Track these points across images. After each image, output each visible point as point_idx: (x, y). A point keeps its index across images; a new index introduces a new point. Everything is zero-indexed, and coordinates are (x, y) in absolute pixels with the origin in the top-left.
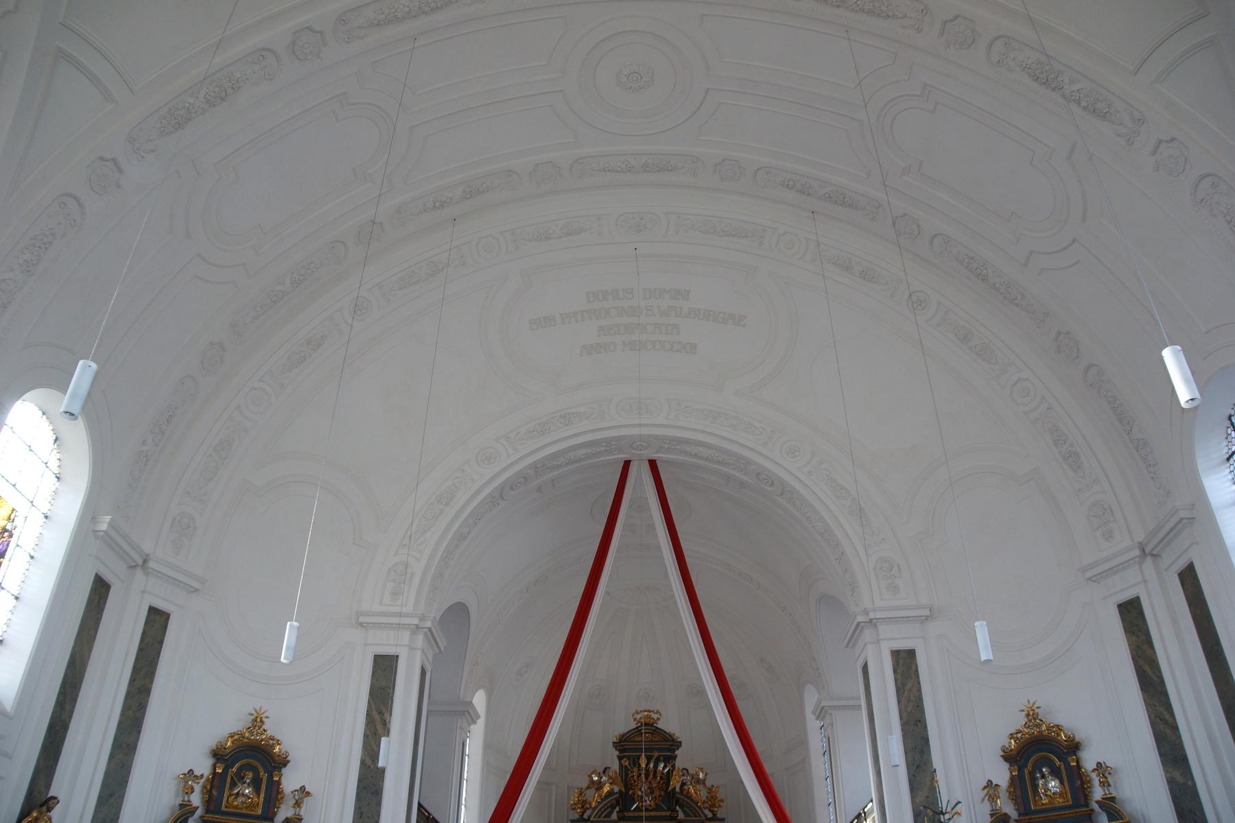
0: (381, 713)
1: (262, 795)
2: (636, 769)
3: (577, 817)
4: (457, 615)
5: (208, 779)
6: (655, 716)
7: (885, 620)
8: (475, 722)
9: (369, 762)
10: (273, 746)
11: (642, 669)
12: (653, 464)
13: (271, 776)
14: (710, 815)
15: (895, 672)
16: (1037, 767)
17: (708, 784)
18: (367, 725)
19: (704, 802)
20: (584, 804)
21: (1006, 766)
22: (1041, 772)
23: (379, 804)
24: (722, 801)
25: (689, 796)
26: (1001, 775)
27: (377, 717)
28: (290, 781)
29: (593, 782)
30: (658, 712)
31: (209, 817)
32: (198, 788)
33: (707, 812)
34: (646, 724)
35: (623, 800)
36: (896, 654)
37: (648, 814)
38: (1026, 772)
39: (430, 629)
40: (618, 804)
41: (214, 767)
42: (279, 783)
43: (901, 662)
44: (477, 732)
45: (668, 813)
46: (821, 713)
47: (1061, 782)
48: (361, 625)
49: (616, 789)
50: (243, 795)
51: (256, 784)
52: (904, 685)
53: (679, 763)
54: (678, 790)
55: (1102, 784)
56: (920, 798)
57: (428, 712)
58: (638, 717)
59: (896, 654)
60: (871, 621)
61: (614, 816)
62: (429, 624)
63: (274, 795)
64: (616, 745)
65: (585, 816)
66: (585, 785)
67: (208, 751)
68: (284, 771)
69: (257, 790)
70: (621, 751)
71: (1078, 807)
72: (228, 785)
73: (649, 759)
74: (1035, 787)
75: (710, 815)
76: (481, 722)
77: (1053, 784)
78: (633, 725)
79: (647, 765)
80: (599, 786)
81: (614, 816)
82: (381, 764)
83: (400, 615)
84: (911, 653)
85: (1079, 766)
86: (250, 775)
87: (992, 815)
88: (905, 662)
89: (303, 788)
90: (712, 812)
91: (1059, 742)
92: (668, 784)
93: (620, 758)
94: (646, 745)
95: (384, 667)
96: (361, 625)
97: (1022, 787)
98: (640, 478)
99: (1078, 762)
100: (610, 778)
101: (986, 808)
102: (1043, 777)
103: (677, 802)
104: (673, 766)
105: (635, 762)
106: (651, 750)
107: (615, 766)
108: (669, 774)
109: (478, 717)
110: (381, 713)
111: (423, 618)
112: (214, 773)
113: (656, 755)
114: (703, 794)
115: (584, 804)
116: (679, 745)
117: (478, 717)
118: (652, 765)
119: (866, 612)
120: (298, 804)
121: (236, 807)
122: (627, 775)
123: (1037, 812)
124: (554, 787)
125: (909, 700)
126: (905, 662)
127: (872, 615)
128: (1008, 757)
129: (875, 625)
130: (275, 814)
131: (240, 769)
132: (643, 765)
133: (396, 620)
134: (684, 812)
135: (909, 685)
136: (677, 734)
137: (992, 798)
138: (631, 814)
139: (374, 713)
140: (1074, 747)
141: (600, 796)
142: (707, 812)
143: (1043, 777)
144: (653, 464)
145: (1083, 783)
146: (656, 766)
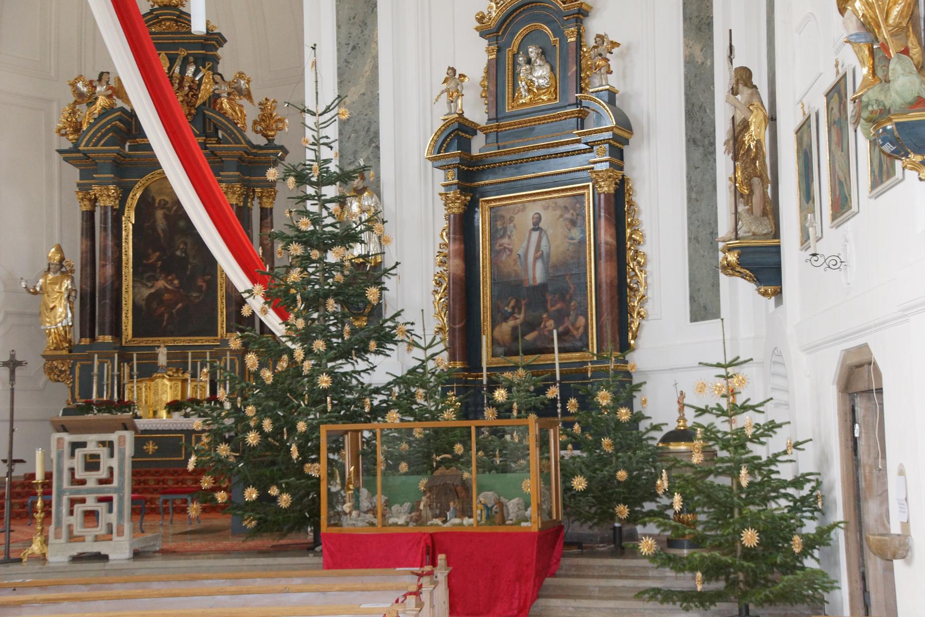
3: (67, 145)
14: (262, 141)
17: (258, 97)
20: (77, 129)
22: (526, 54)
26: (475, 58)
29: (80, 95)
47: (552, 69)
56: (353, 95)
66: (72, 99)
73: (172, 60)
79: (170, 69)
80: (91, 100)
85: (579, 44)
90: (266, 136)
99: (580, 36)
102: (529, 62)
106: (176, 46)
113: (183, 53)
114: (251, 112)
118: (177, 70)
141: (91, 114)
146: (183, 71)
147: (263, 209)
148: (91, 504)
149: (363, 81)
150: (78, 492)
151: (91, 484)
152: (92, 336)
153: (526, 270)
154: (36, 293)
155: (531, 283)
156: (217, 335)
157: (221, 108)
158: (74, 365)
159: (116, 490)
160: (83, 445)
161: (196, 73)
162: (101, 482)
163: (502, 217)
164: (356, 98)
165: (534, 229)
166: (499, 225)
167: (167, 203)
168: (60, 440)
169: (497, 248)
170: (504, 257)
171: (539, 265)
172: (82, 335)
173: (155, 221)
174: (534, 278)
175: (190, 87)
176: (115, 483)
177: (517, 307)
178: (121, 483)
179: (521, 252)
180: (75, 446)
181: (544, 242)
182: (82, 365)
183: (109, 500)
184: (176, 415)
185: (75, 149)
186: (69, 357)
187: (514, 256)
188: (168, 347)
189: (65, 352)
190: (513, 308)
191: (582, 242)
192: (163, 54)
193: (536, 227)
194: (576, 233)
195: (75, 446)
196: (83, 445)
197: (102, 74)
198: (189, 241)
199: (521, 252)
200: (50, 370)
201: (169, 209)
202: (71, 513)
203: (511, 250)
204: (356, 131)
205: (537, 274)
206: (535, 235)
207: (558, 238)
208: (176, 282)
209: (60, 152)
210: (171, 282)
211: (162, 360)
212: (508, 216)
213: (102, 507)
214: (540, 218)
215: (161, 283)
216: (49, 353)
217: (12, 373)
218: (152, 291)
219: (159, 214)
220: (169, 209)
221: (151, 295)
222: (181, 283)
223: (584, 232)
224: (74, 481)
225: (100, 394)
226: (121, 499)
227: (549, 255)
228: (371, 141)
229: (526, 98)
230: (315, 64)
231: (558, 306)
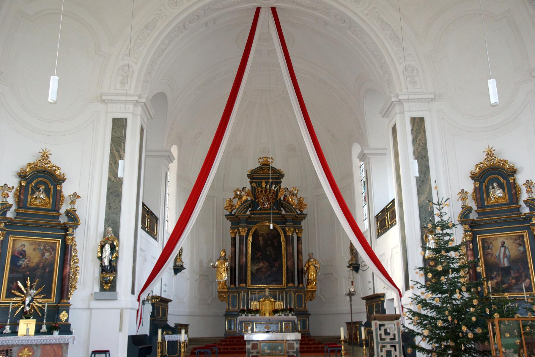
0: (118, 151)
1: (51, 198)
2: (259, 188)
3: (228, 213)
4: (160, 99)
5: (17, 190)
6: (270, 160)
7: (408, 100)
8: (172, 162)
9: (113, 179)
10: (55, 171)
11: (265, 133)
12: (274, 10)
13: (55, 187)
14: (299, 212)
15: (412, 129)
16: (491, 182)
17: (299, 196)
18: (110, 158)
19: (296, 206)
21: (473, 181)
22: (492, 185)
23: (120, 201)
24: (306, 205)
25: (288, 202)
26: (470, 186)
27: (116, 154)
28: (67, 190)
30: (272, 158)
31: (20, 211)
32: (11, 194)
33: (297, 210)
34: (266, 165)
35: (253, 204)
36: (413, 120)
37: (269, 212)
38: (484, 185)
39: (144, 103)
40: (250, 207)
41: (21, 184)
42: (61, 191)
43: (416, 124)
44: (173, 167)
45: (277, 211)
46: (363, 157)
47: (504, 191)
48: (104, 101)
49: (249, 199)
50: (39, 198)
51: (47, 192)
52: (416, 137)
53: (283, 186)
54: (282, 199)
55: (528, 192)
56: (423, 198)
57: (146, 156)
58: (261, 161)
59: (413, 120)
60: (400, 100)
61: (248, 213)
62: (144, 100)
63: (57, 198)
64: (249, 176)
65: (233, 213)
67: (16, 174)
68: (63, 184)
69: (48, 195)
70: (251, 179)
71: (512, 204)
72: (30, 192)
73: (267, 183)
74: (488, 194)
75: (299, 212)
76: (175, 162)
77: (499, 193)
78: (258, 165)
79: (266, 186)
80: (240, 197)
81: (248, 213)
82: (120, 175)
83: (126, 95)
84: (422, 119)
86: (43, 187)
87: (463, 208)
88: (418, 125)
89: (75, 194)
91: (504, 169)
92: (277, 196)
93: (251, 183)
94: (265, 176)
95: (119, 126)
96: (104, 101)
97: (480, 194)
98: (266, 17)
99: (514, 180)
100: (246, 193)
101: (460, 204)
102: (493, 188)
103: (282, 206)
104: (280, 187)
105: (259, 184)
107: (249, 187)
108: (278, 191)
109: (174, 159)
110: (118, 151)
111: (140, 97)
112: (21, 186)
114: (296, 202)
115: (232, 207)
116: (283, 176)
117: (174, 159)
118: (268, 186)
119: (397, 95)
120: (73, 202)
121: (36, 205)
122: (255, 191)
123: (488, 206)
124: (215, 199)
125: (419, 145)
126: (418, 125)
127: (401, 97)
128: (474, 177)
129: (402, 103)
130: (60, 208)
131: (37, 183)
132: (264, 186)
133: (124, 98)
134: (285, 211)
135: (420, 137)
136: (282, 170)
137: (463, 199)
138: (257, 212)
139: (115, 151)
140: (513, 172)
142: (297, 210)
143: (493, 188)
144: (274, 10)
145: (516, 192)
147: (298, 237)
148: (388, 348)
149: (426, 193)
150: (384, 343)
151: (388, 340)
152: (235, 284)
153: (500, 261)
154: (215, 267)
155: (503, 266)
156: (282, 284)
157: (288, 200)
158: (229, 295)
159: (397, 343)
160: (383, 325)
161: (275, 188)
162: (391, 339)
163: (487, 242)
164: (424, 199)
165: (502, 247)
166: (486, 245)
167: (263, 234)
168: (376, 323)
169: (486, 253)
170: (489, 256)
171: (506, 260)
172: (231, 284)
173: (259, 241)
174: (504, 264)
175: (273, 193)
176: (397, 340)
177: (498, 274)
178: (399, 340)
179: (497, 255)
180: (381, 326)
181: (507, 251)
182: (232, 296)
183: (394, 346)
184: (276, 315)
185: (231, 214)
186: (228, 292)
187: (494, 256)
188: (269, 289)
189: (226, 290)
190: (496, 275)
191: (525, 252)
192: (264, 181)
193: (503, 245)
194: (521, 248)
195: (381, 326)
196: (383, 325)
197: (244, 188)
198: (272, 249)
199: (497, 255)
200: (220, 297)
201: (264, 237)
202: (382, 351)
203: (492, 254)
204: (425, 211)
205: (506, 263)
206: (503, 249)
207: (513, 250)
208: (267, 264)
209: (226, 215)
210: (265, 264)
211: (267, 293)
212: (489, 242)
213: (393, 349)
214: (504, 243)
215: (261, 265)
216: (220, 290)
217: (351, 298)
218: (258, 267)
219: (261, 238)
220: (264, 237)
221: (257, 269)
222: (269, 264)
223: (525, 247)
224: (382, 339)
225: (244, 306)
226: (400, 346)
227: (510, 256)
228: (431, 214)
229: (493, 200)
230: (436, 188)
231: (516, 275)
